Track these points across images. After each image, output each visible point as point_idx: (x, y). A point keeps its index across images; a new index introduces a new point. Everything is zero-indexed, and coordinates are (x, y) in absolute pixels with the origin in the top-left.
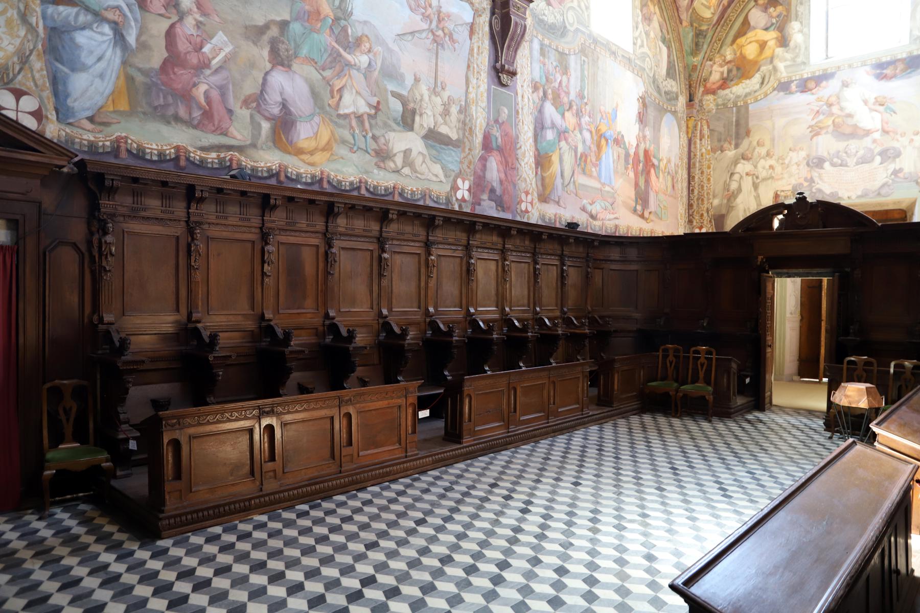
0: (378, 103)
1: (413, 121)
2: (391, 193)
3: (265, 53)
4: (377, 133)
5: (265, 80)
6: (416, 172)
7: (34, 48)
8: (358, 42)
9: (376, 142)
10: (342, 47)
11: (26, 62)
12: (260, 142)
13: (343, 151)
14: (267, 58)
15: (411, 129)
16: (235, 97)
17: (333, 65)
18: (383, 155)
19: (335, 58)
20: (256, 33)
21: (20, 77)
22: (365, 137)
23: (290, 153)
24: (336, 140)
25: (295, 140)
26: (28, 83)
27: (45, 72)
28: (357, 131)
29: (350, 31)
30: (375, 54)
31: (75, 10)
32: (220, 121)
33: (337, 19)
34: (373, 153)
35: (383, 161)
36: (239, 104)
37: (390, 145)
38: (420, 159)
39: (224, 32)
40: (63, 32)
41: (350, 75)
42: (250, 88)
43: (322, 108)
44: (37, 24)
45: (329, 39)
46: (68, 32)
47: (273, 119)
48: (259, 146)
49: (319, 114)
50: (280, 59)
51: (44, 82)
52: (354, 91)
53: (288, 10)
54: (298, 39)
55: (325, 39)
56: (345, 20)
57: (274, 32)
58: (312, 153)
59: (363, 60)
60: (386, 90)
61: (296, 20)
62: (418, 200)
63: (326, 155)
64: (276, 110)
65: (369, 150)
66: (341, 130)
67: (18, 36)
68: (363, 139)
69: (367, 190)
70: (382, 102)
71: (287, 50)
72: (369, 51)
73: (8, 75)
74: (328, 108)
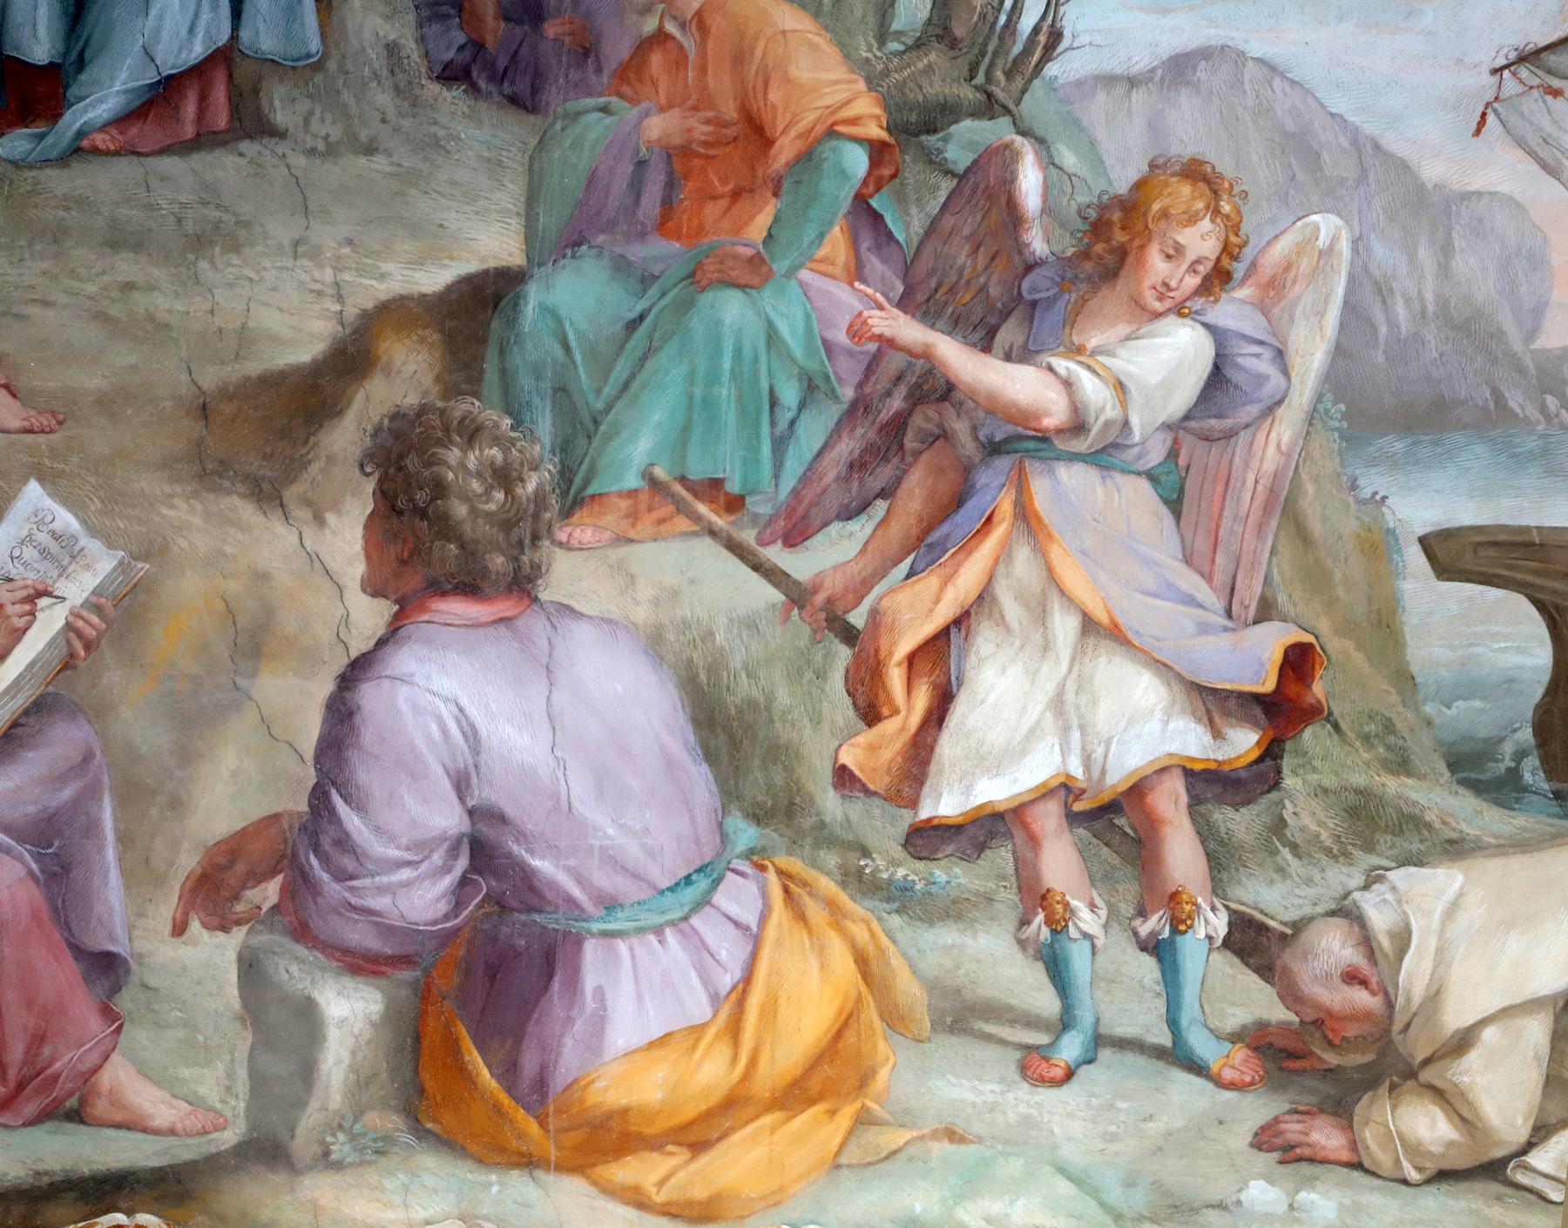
0: (1298, 661)
3: (345, 540)
4: (1273, 897)
5: (341, 714)
8: (1111, 240)
9: (1266, 971)
10: (957, 326)
12: (310, 1121)
13: (965, 1084)
14: (359, 569)
16: (141, 873)
17: (883, 475)
19: (898, 425)
20: (264, 428)
22: (1156, 948)
23: (528, 1162)
24: (894, 1018)
25: (569, 1062)
28: (1088, 920)
29: (1030, 182)
30: (1275, 287)
32: (38, 1039)
33: (914, 127)
35: (1341, 1109)
36: (165, 910)
37: (1414, 974)
39: (47, 478)
41: (1025, 515)
42: (231, 791)
43: (782, 811)
45: (845, 301)
47: (404, 960)
48: (303, 1142)
49: (757, 858)
50: (448, 548)
52: (1065, 626)
53: (510, 196)
54: (584, 376)
55: (830, 300)
56: (990, 107)
57: (407, 375)
58: (697, 1134)
59: (1158, 362)
60: (1377, 545)
61: (573, 242)
63: (818, 1131)
64: (423, 899)
65: (1203, 1045)
66: (947, 935)
68: (1147, 968)
70: (1334, 644)
71: (504, 477)
72: (1218, 278)
74: (830, 803)
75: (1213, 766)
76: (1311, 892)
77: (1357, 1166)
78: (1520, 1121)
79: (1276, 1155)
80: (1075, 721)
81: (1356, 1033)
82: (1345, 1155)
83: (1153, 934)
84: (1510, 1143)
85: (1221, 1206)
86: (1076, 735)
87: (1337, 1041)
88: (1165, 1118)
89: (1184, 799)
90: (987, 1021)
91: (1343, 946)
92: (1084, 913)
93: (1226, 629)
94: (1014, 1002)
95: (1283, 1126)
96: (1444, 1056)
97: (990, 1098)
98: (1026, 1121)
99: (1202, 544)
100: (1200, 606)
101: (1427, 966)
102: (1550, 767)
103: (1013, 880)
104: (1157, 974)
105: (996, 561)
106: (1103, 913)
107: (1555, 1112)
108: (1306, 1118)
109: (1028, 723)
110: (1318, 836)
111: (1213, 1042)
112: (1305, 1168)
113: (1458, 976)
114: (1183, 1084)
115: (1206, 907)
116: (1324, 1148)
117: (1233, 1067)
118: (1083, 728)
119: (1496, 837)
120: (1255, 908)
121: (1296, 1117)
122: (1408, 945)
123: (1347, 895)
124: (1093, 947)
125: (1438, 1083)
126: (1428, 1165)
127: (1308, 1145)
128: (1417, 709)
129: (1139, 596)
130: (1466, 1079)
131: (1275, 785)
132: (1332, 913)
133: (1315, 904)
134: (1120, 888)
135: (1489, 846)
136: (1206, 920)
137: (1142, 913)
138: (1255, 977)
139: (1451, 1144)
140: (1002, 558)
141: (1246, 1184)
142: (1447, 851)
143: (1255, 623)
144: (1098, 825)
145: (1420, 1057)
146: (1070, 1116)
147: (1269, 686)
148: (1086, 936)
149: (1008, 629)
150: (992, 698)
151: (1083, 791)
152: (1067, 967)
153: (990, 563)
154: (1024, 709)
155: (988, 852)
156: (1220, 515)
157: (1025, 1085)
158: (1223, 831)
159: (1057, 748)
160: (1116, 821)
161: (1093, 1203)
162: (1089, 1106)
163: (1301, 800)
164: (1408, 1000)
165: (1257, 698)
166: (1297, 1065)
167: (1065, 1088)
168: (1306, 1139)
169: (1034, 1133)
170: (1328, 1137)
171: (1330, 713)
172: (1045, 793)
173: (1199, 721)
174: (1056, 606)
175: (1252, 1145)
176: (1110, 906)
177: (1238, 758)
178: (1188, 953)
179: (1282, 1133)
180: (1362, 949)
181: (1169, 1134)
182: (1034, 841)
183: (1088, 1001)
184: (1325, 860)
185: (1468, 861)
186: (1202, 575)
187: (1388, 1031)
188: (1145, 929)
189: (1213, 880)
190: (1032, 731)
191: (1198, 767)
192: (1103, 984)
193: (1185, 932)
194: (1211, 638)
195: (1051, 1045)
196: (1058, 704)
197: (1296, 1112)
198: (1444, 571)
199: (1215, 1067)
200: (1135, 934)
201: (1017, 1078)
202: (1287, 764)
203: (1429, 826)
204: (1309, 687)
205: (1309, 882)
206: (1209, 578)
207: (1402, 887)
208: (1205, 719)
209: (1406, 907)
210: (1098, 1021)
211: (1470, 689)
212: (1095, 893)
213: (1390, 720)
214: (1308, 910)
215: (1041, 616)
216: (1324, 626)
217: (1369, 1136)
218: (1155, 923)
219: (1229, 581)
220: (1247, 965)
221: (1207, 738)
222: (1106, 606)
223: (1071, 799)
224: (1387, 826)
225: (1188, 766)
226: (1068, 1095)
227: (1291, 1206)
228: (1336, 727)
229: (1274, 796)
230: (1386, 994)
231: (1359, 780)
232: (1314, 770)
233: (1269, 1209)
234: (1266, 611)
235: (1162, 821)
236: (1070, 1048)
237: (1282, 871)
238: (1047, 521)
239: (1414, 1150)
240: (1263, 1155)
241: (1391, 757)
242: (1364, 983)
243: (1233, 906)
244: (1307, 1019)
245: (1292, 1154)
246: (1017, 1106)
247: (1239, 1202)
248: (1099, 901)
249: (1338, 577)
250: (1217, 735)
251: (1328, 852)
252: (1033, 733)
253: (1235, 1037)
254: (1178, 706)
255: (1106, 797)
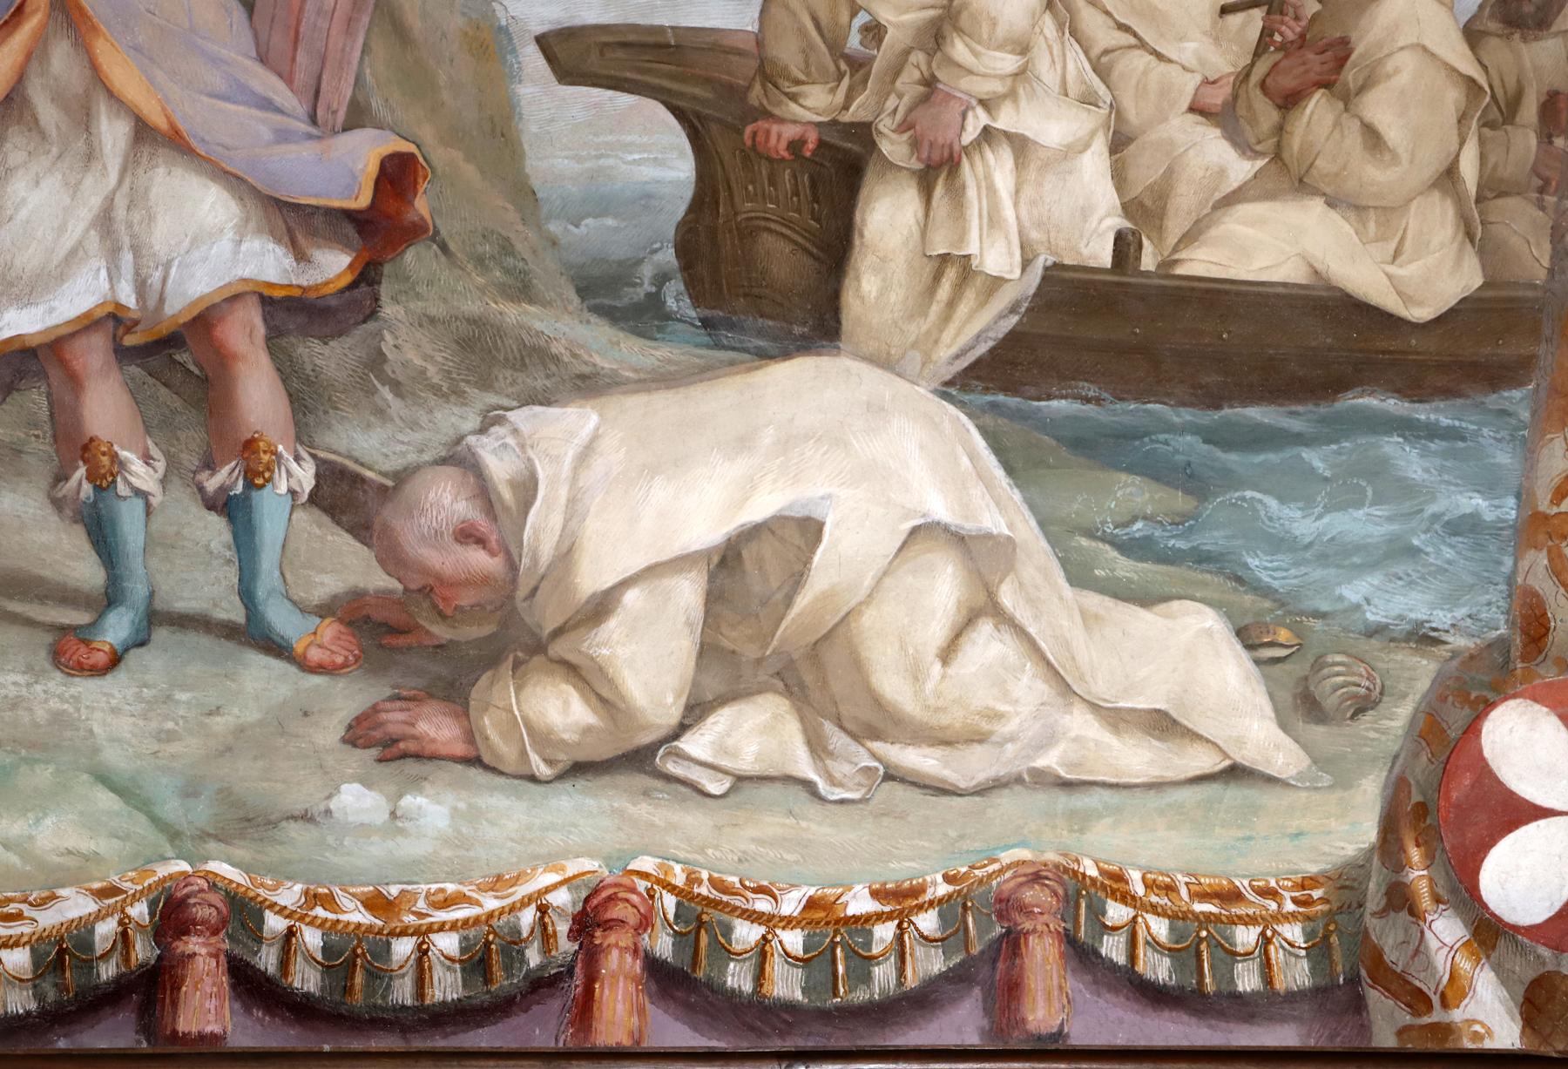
0: (398, 175)
1: (835, 248)
2: (542, 985)
4: (369, 444)
6: (879, 723)
9: (362, 530)
15: (815, 321)
18: (442, 645)
28: (141, 474)
34: (326, 640)
35: (453, 692)
37: (542, 528)
38: (942, 587)
52: (113, 133)
60: (489, 43)
62: (921, 1001)
65: (283, 620)
68: (215, 530)
69: (248, 984)
70: (440, 155)
75: (297, 293)
76: (417, 436)
77: (474, 761)
78: (670, 700)
79: (374, 752)
80: (126, 241)
81: (473, 601)
82: (460, 749)
83: (223, 489)
84: (660, 727)
85: (306, 817)
86: (127, 258)
87: (449, 612)
88: (236, 711)
89: (261, 330)
90: (11, 597)
91: (455, 500)
92: (137, 466)
93: (310, 137)
94: (46, 573)
95: (384, 716)
96: (576, 626)
97: (12, 691)
98: (57, 718)
99: (279, 42)
100: (279, 111)
101: (556, 520)
102: (697, 291)
103: (47, 427)
104: (227, 537)
105: (29, 56)
106: (161, 465)
107: (713, 685)
108: (411, 705)
109: (68, 242)
110: (423, 372)
111: (296, 617)
112: (411, 767)
113: (593, 529)
114: (262, 679)
115: (288, 456)
116: (433, 741)
117: (320, 646)
118: (136, 250)
119: (636, 371)
120: (349, 457)
121: (398, 704)
122: (534, 497)
123: (459, 440)
124: (148, 506)
125: (570, 657)
126: (562, 756)
127: (414, 737)
128: (539, 227)
129: (205, 99)
130: (604, 651)
131: (373, 314)
132: (443, 462)
133: (421, 451)
134: (182, 436)
135: (628, 381)
136: (288, 472)
137: (210, 465)
138: (348, 538)
139: (588, 730)
140: (35, 54)
141: (337, 789)
142: (579, 389)
143: (344, 130)
144: (155, 362)
145: (549, 627)
146: (115, 711)
147: (363, 200)
148: (138, 492)
149: (43, 136)
150: (23, 214)
151: (136, 323)
152: (114, 531)
153: (21, 58)
154: (62, 229)
155: (16, 395)
156: (301, 9)
157: (58, 676)
158: (309, 367)
159: (103, 273)
160: (177, 357)
161: (143, 818)
162: (139, 698)
163: (403, 331)
164: (535, 560)
165: (349, 215)
166: (401, 641)
167: (109, 677)
168: (409, 730)
169: (68, 734)
170: (438, 728)
171: (436, 232)
172: (88, 324)
173: (278, 241)
174: (103, 108)
175: (344, 740)
176: (168, 456)
177: (327, 283)
178: (265, 511)
179: (381, 724)
180: (478, 502)
181: (240, 730)
182: (75, 382)
183: (141, 571)
184: (433, 400)
185: (603, 399)
186: (280, 76)
187: (511, 598)
188: (212, 484)
189: (296, 424)
190: (73, 252)
191: (278, 294)
192: (159, 550)
193: (262, 487)
194: (293, 147)
195: (93, 624)
196: (105, 221)
197: (399, 698)
198: (567, 73)
199: (299, 648)
200: (201, 489)
201: (48, 666)
202: (385, 290)
203: (556, 359)
204: (411, 203)
205: (414, 425)
206: (288, 79)
207: (525, 428)
208: (286, 239)
209: (530, 453)
210: (152, 594)
211: (602, 205)
212: (149, 442)
213: (507, 239)
214: (412, 458)
215: (83, 119)
216: (427, 134)
217: (489, 724)
218: (225, 477)
219: (313, 82)
220: (338, 523)
221: (289, 261)
222: (164, 109)
223: (121, 331)
224: (506, 359)
225: (266, 292)
226: (116, 686)
227: (393, 815)
228: (444, 248)
229: (371, 326)
230: (508, 553)
231: (472, 307)
232: (418, 296)
233: (365, 819)
234: (358, 116)
235: (235, 357)
236: (117, 628)
237: (381, 413)
238: (91, 12)
239: (543, 739)
240: (358, 751)
241: (510, 281)
242: (481, 542)
243: (322, 454)
244: (413, 586)
245: (394, 750)
246: (46, 701)
247: (328, 812)
248: (155, 452)
249: (442, 79)
250: (301, 256)
251: (436, 390)
252: (74, 255)
253: (324, 610)
254: (252, 225)
255: (164, 330)
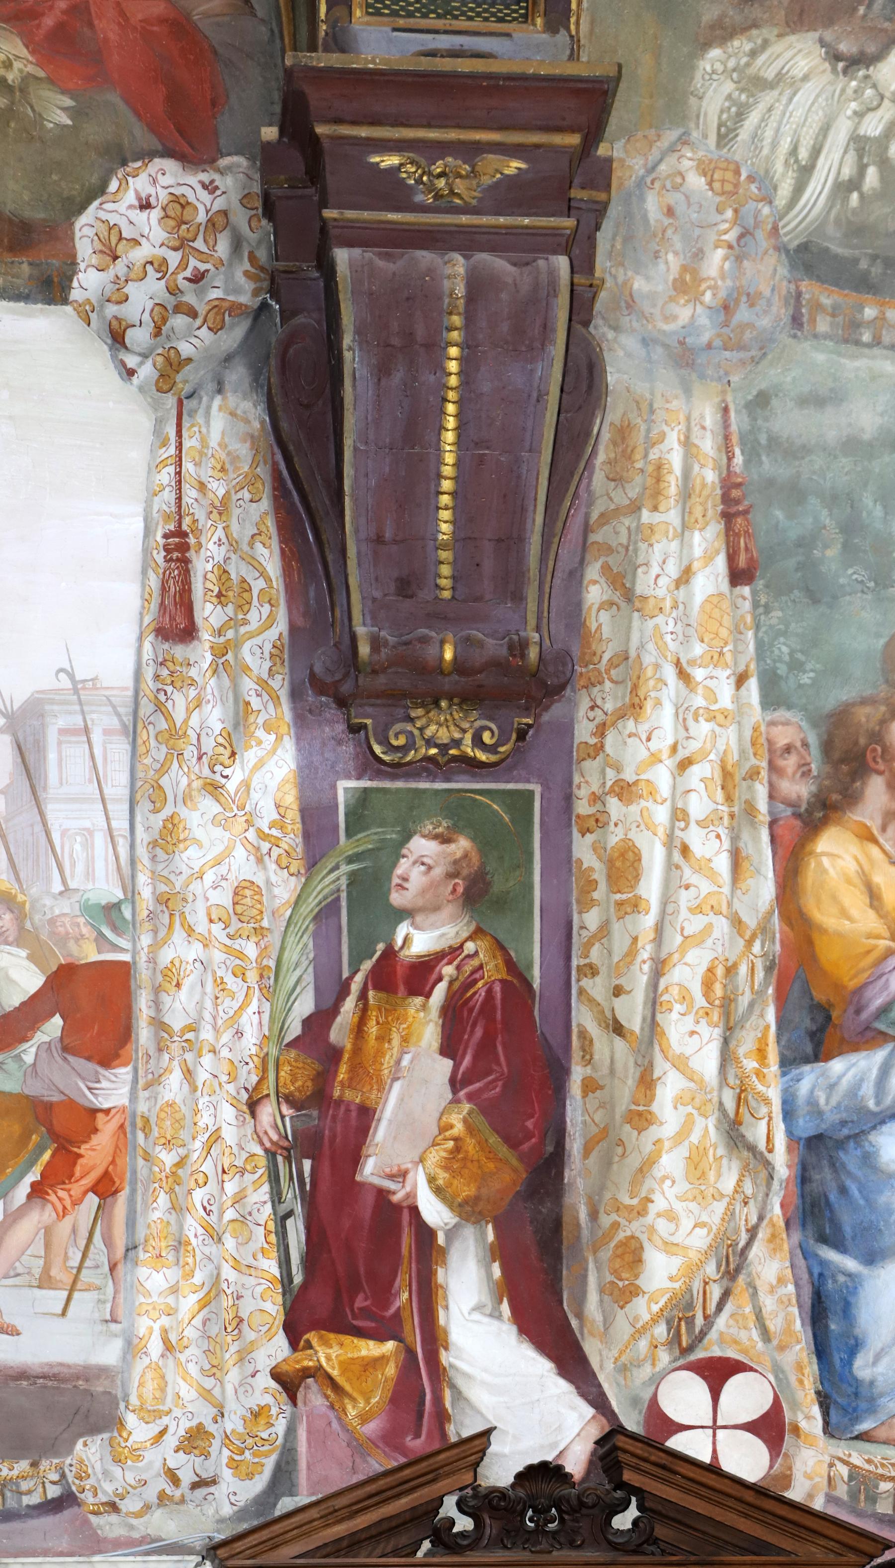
7: (761, 1218)
11: (738, 1270)
21: (722, 1322)
26: (743, 1336)
27: (791, 1288)
31: (880, 1055)
40: (841, 1144)
44: (769, 1139)
46: (858, 1137)
51: (789, 1322)
67: (718, 1196)
73: (690, 1321)
